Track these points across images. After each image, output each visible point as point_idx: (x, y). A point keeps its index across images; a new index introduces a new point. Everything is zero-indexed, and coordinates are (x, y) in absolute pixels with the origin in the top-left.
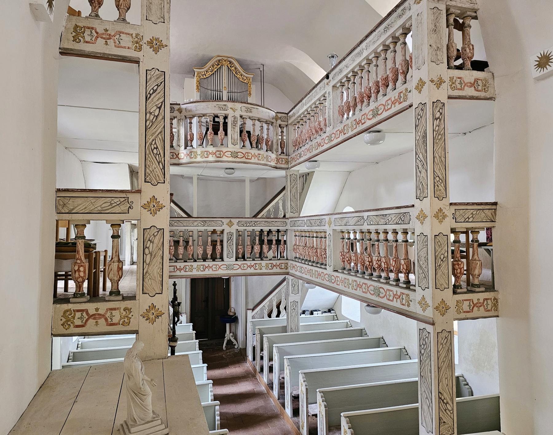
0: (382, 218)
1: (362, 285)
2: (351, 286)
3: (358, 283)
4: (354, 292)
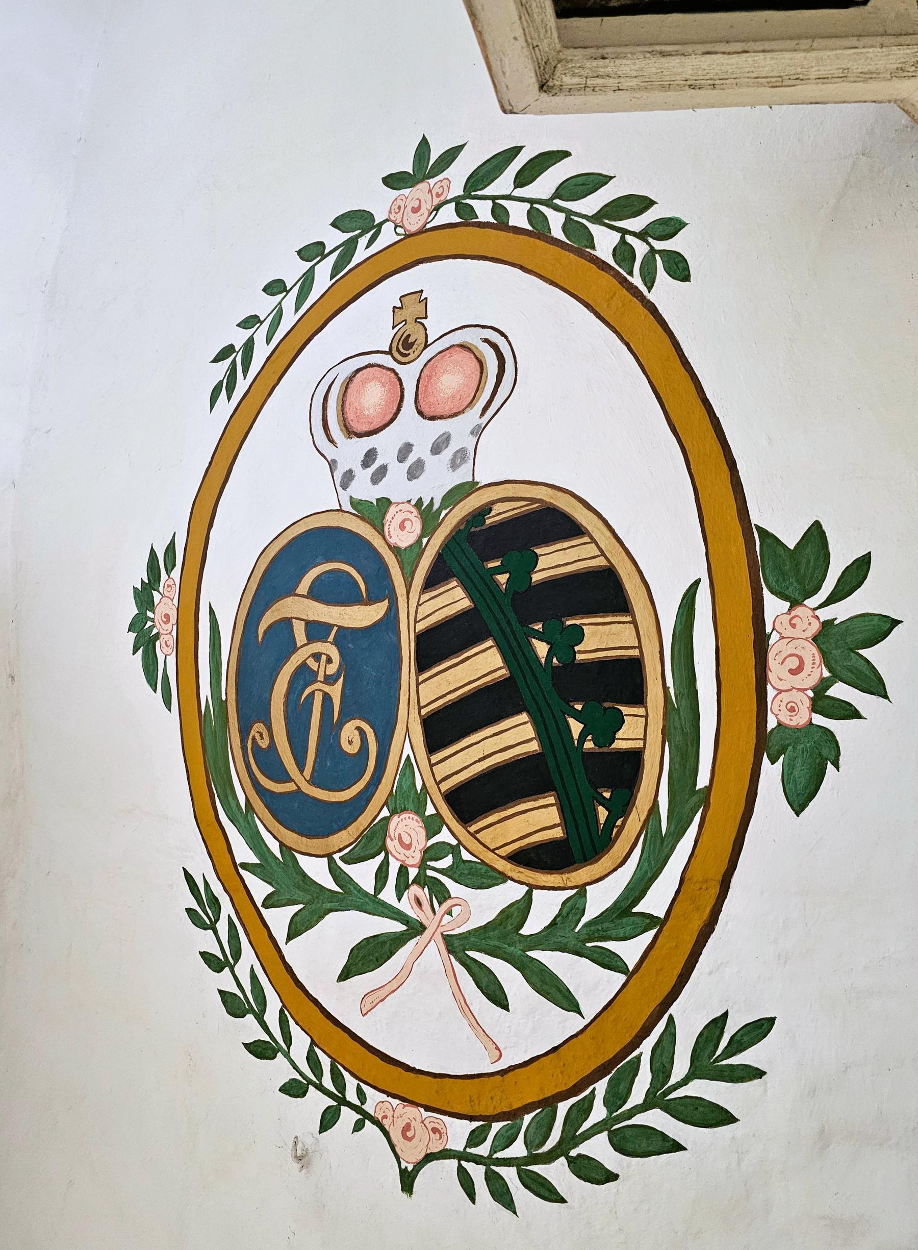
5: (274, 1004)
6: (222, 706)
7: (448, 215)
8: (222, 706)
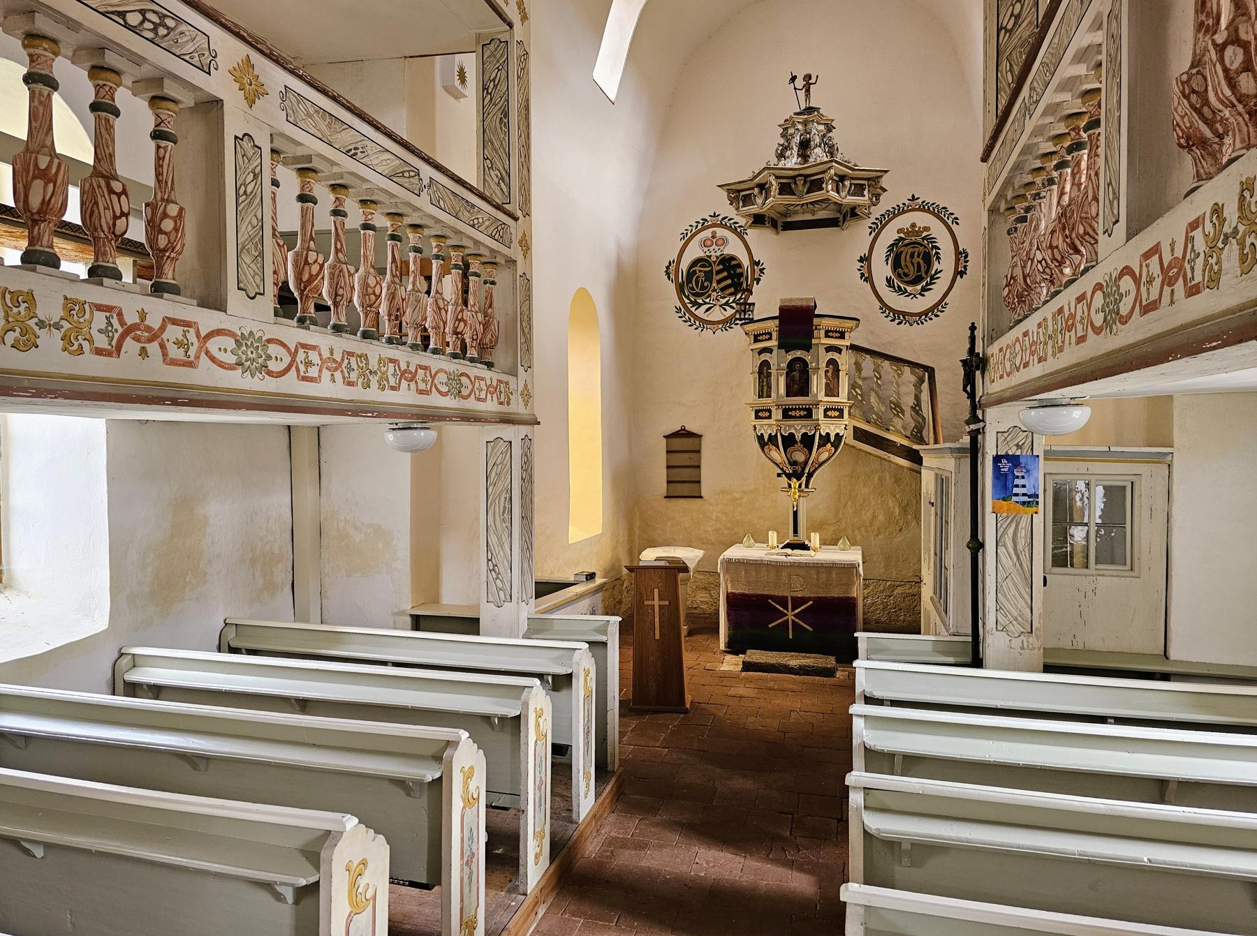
0: (466, 209)
1: (416, 371)
3: (403, 367)
4: (389, 397)
5: (692, 319)
7: (719, 222)
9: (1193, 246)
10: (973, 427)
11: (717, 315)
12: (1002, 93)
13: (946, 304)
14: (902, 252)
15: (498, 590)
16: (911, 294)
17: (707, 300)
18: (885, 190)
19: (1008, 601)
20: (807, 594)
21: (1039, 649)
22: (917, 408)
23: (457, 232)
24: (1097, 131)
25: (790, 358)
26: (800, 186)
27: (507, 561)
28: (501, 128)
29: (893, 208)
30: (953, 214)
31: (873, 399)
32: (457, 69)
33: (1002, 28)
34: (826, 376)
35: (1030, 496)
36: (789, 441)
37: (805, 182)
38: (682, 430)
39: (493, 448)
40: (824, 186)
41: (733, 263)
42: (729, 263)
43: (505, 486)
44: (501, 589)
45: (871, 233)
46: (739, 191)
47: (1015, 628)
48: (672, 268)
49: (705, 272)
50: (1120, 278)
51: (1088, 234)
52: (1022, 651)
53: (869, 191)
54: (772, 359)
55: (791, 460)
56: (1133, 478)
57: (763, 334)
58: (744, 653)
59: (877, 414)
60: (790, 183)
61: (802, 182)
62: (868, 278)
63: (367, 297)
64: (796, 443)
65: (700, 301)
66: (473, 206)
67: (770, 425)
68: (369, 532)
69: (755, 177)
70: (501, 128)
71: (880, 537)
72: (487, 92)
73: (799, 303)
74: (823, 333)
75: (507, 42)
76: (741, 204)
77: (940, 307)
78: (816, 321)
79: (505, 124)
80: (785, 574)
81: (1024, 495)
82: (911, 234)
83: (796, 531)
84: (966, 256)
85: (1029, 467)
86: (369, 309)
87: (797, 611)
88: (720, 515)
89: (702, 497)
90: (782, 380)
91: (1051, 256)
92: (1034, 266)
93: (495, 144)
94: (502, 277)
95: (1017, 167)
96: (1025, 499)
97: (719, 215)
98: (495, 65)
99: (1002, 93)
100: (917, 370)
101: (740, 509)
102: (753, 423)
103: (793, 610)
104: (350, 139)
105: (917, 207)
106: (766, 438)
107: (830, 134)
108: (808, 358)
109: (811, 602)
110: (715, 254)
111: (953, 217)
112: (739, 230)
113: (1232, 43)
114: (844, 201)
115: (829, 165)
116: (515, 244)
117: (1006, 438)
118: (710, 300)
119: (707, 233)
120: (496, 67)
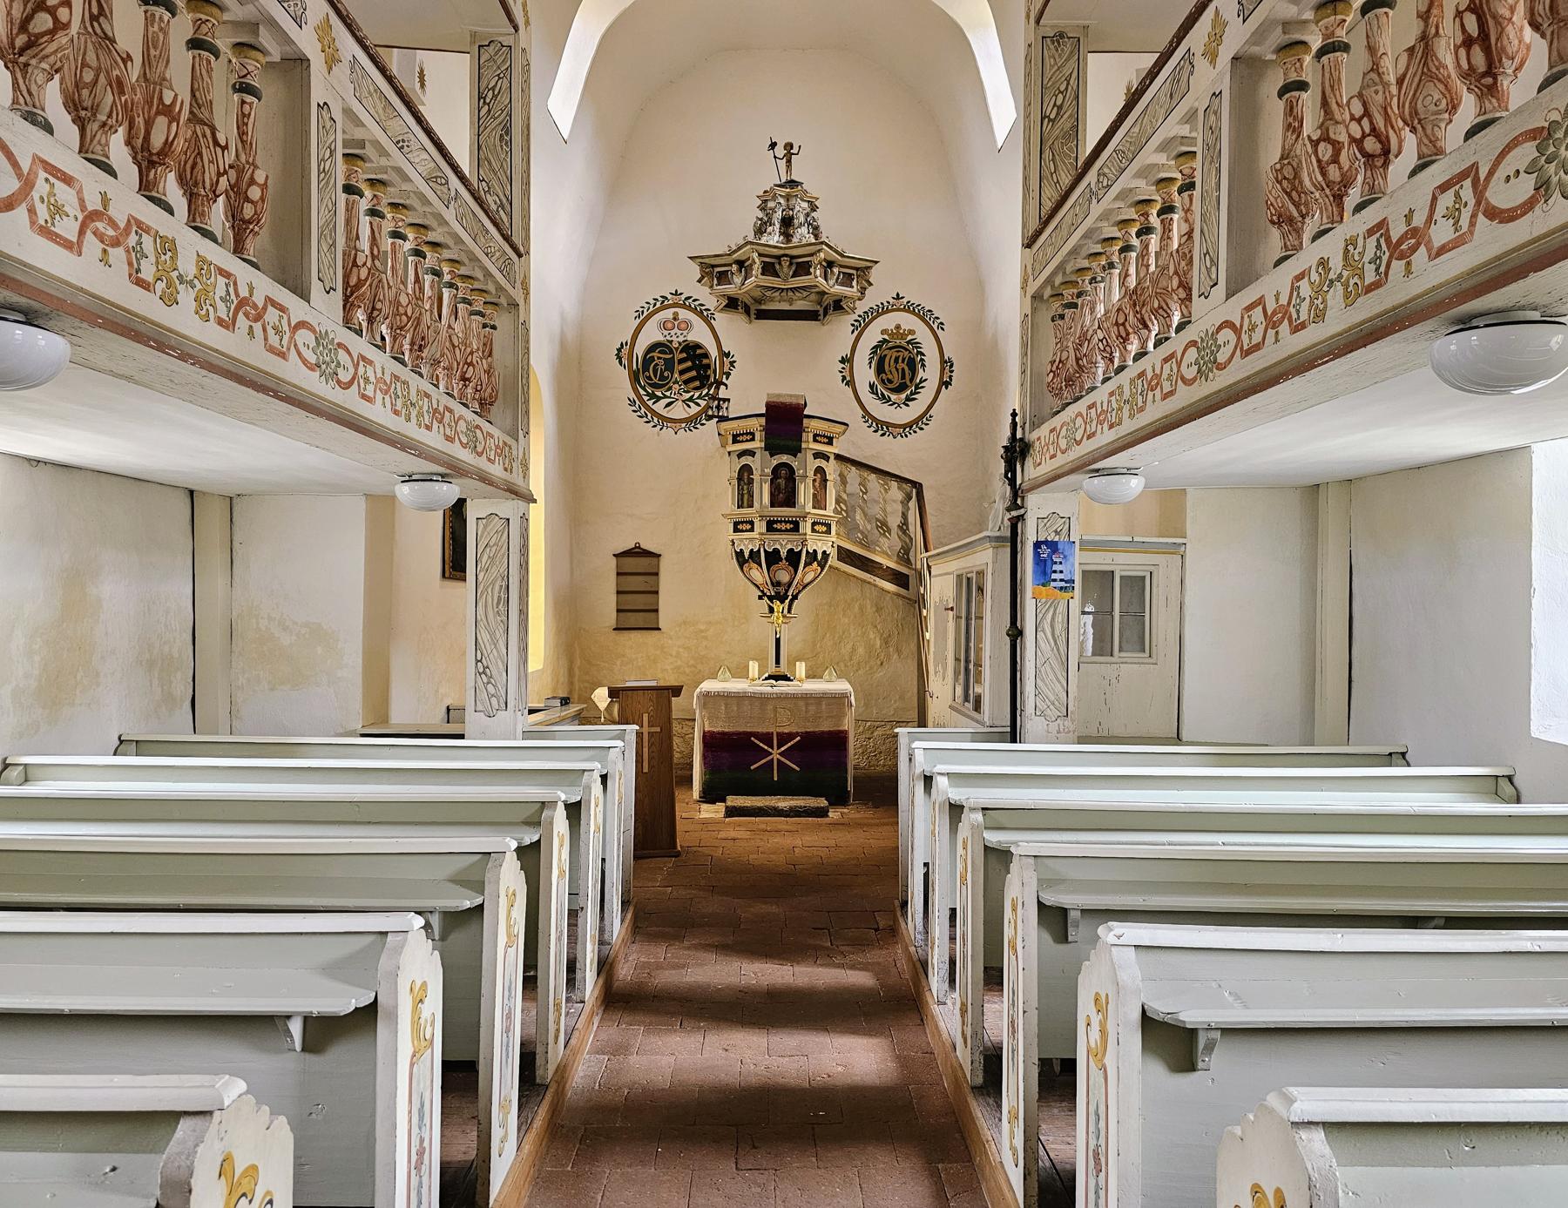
1: (444, 412)
2: (414, 413)
5: (649, 415)
6: (638, 369)
8: (638, 369)
9: (1299, 293)
10: (1014, 513)
11: (679, 411)
12: (1045, 181)
13: (930, 417)
14: (886, 355)
15: (490, 696)
16: (895, 403)
17: (668, 394)
18: (870, 284)
19: (1046, 685)
20: (794, 729)
21: (1074, 732)
22: (905, 527)
23: (474, 259)
24: (1169, 216)
25: (775, 463)
26: (785, 268)
27: (503, 662)
28: (501, 146)
29: (877, 306)
30: (938, 318)
31: (859, 516)
32: (418, 69)
33: (1046, 117)
34: (814, 486)
35: (1066, 582)
36: (773, 558)
37: (791, 264)
38: (636, 547)
39: (485, 527)
40: (812, 270)
41: (699, 351)
42: (693, 352)
43: (501, 571)
44: (493, 696)
45: (853, 332)
46: (713, 266)
47: (1052, 713)
48: (625, 351)
49: (664, 359)
50: (1217, 333)
51: (1162, 308)
52: (1058, 735)
53: (858, 282)
54: (754, 463)
55: (774, 581)
56: (1152, 568)
57: (743, 434)
58: (724, 801)
59: (862, 533)
60: (773, 264)
61: (788, 263)
62: (850, 383)
63: (398, 317)
64: (781, 560)
65: (659, 394)
66: (487, 232)
67: (751, 540)
68: (303, 632)
69: (735, 251)
70: (501, 146)
71: (860, 672)
72: (484, 102)
73: (788, 400)
74: (811, 436)
75: (511, 47)
76: (715, 282)
77: (924, 419)
78: (805, 421)
79: (507, 143)
80: (770, 707)
81: (1061, 580)
82: (895, 336)
83: (778, 661)
84: (951, 366)
85: (1066, 553)
86: (398, 331)
87: (783, 749)
88: (681, 650)
89: (660, 629)
90: (766, 488)
91: (1116, 333)
92: (1091, 346)
93: (494, 163)
94: (502, 320)
95: (1074, 252)
96: (1063, 584)
97: (681, 294)
98: (495, 71)
99: (1045, 181)
100: (904, 486)
101: (704, 643)
102: (731, 538)
103: (778, 748)
104: (398, 128)
105: (902, 307)
106: (747, 555)
107: (813, 214)
108: (795, 465)
109: (799, 738)
110: (677, 340)
111: (939, 321)
112: (705, 313)
113: (1324, 140)
114: (832, 290)
115: (818, 247)
116: (518, 285)
117: (1045, 525)
118: (671, 394)
119: (668, 314)
120: (498, 73)
